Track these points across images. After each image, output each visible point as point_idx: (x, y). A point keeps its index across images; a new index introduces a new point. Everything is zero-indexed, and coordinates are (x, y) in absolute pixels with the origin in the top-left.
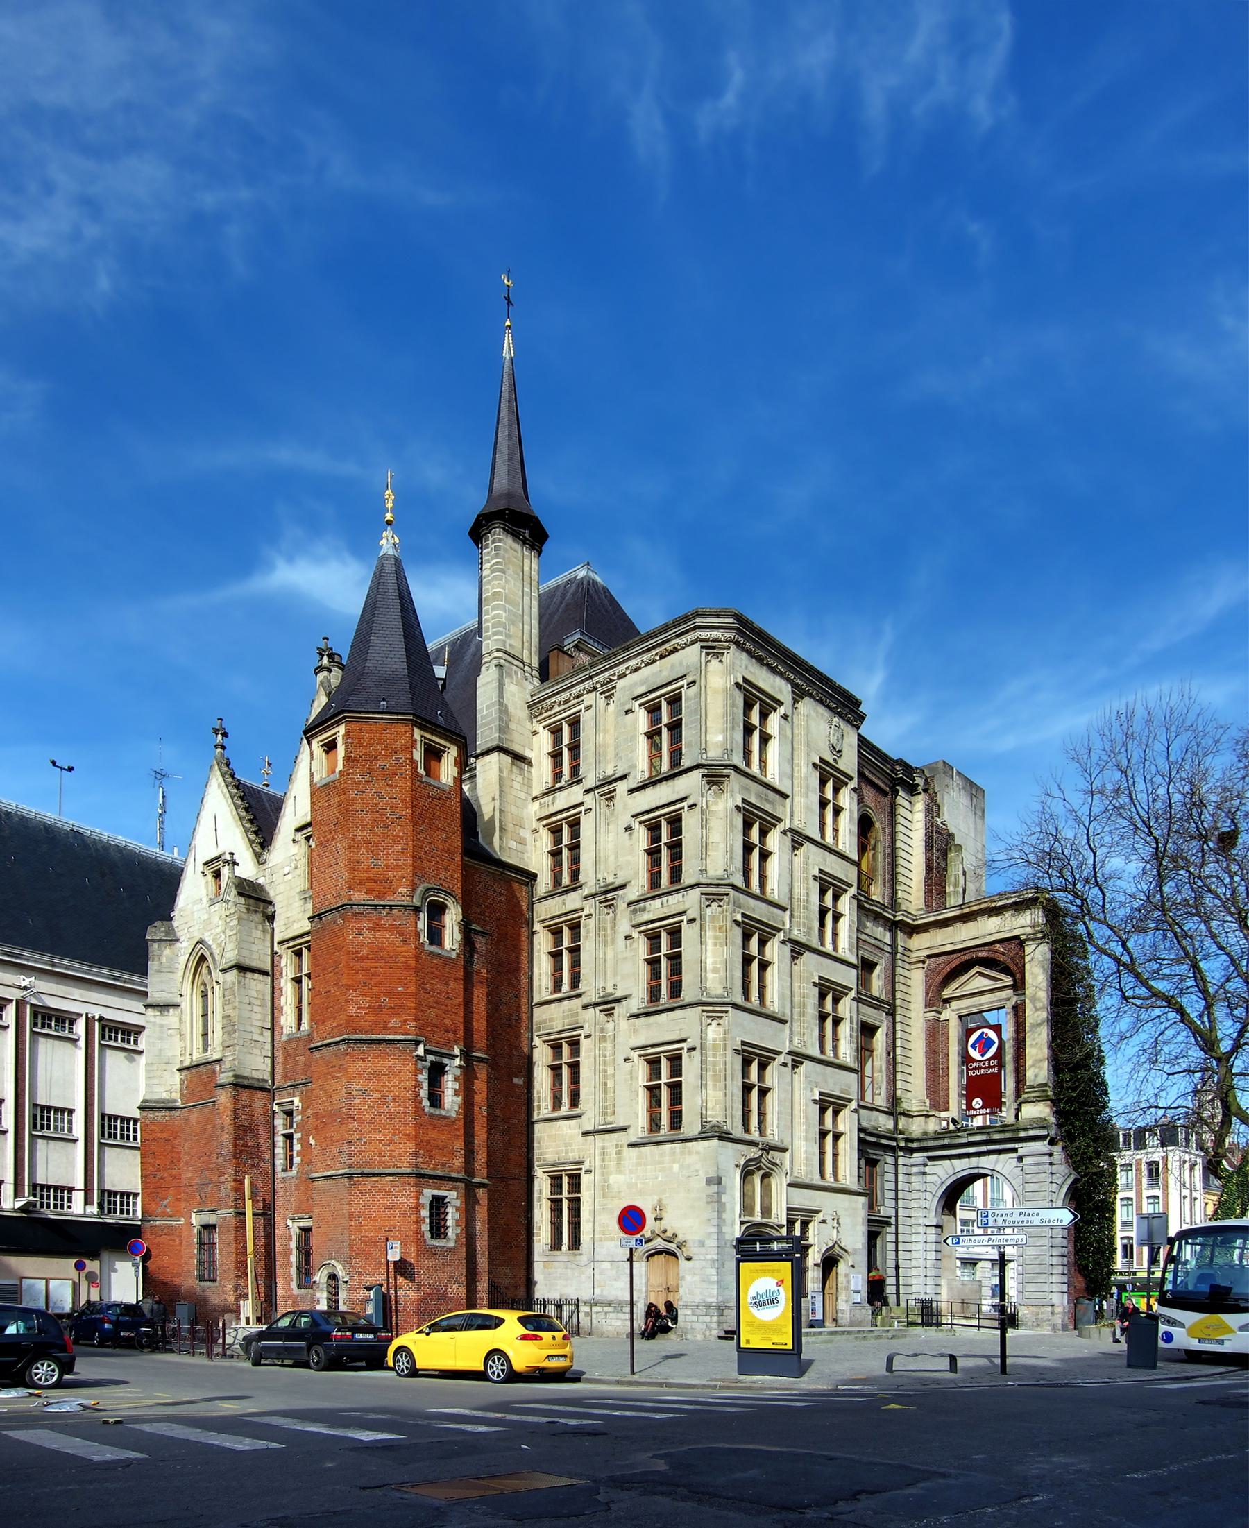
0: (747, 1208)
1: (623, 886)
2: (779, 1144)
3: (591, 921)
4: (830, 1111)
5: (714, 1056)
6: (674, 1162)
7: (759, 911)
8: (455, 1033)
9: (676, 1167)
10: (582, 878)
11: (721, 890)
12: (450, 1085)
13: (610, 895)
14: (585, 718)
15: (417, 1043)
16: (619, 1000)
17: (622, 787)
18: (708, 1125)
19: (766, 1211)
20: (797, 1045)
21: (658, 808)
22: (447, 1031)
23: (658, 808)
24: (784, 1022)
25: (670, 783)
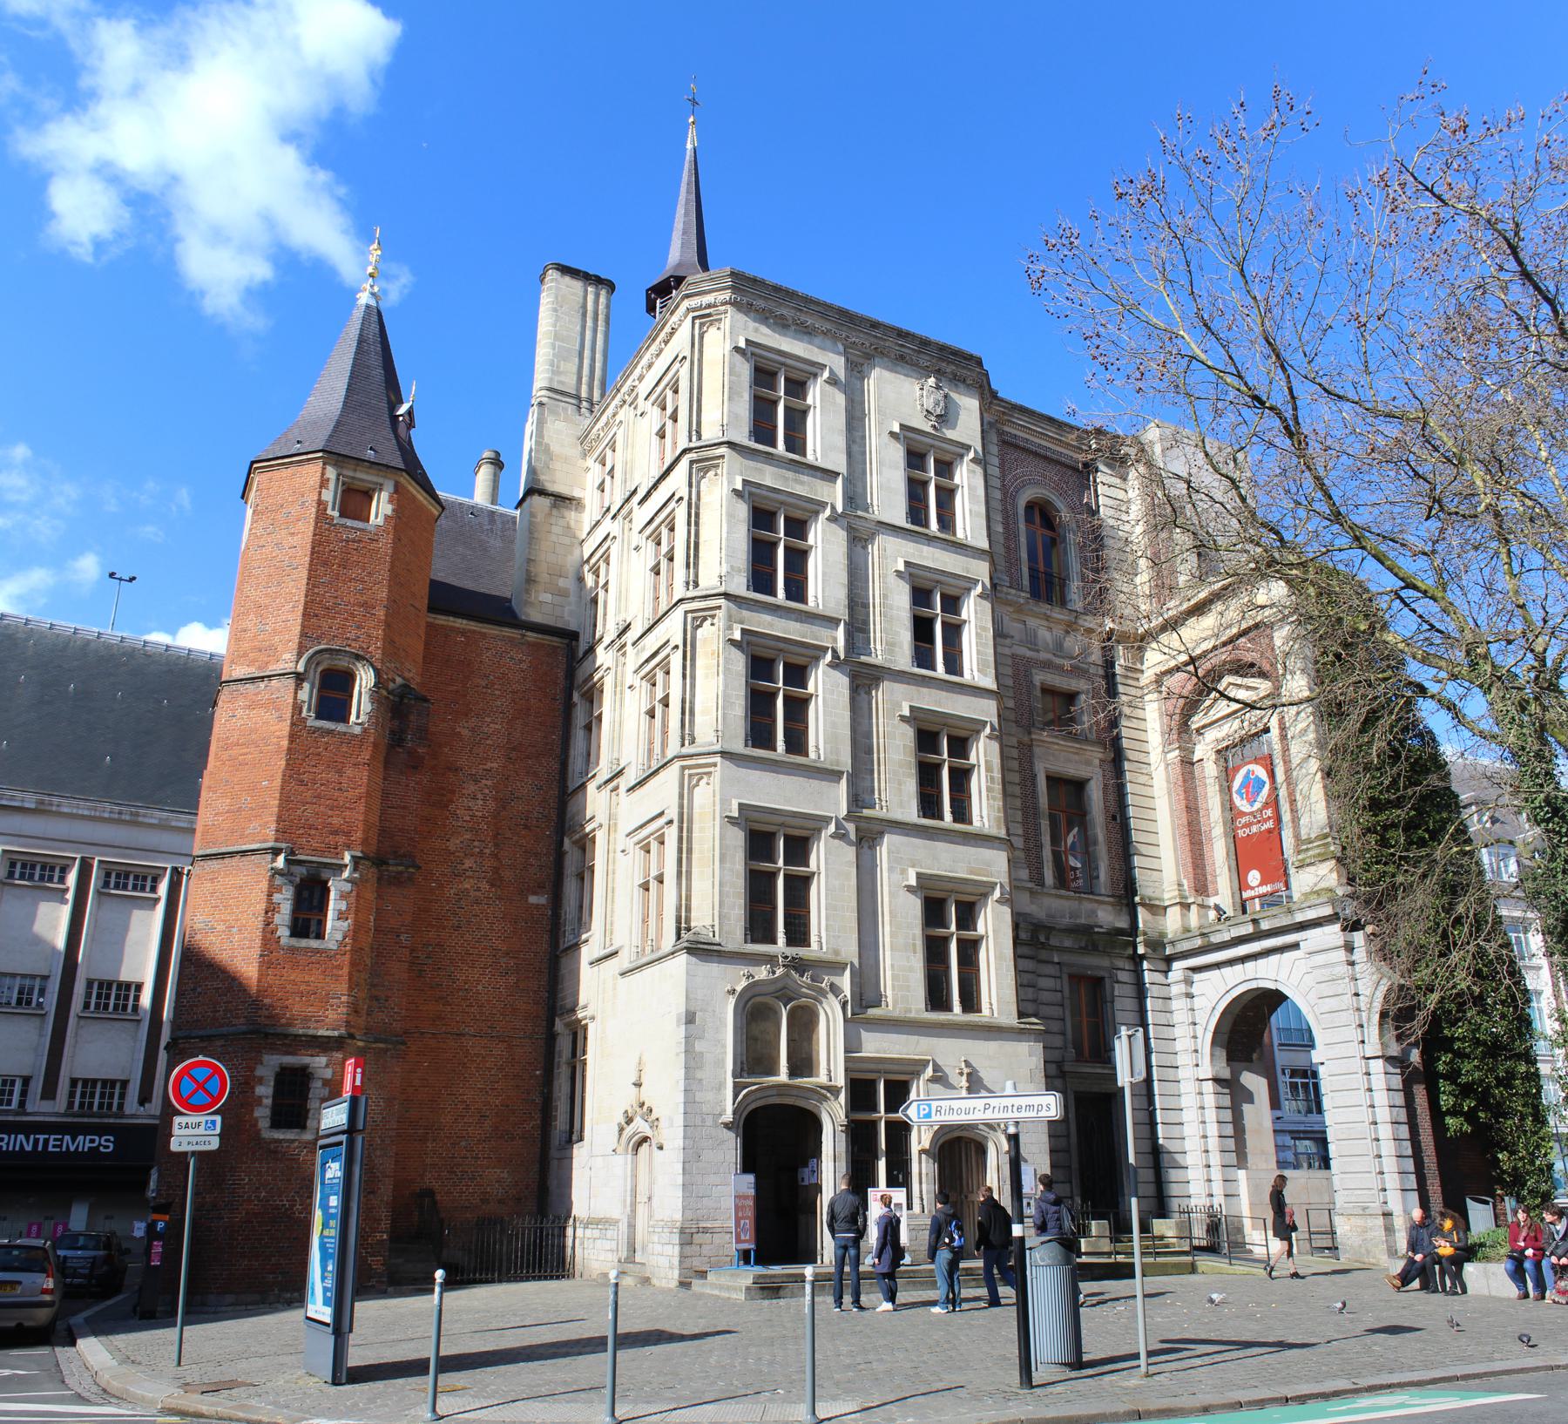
0: (754, 1058)
2: (830, 957)
8: (348, 834)
15: (276, 852)
19: (802, 1063)
22: (335, 833)
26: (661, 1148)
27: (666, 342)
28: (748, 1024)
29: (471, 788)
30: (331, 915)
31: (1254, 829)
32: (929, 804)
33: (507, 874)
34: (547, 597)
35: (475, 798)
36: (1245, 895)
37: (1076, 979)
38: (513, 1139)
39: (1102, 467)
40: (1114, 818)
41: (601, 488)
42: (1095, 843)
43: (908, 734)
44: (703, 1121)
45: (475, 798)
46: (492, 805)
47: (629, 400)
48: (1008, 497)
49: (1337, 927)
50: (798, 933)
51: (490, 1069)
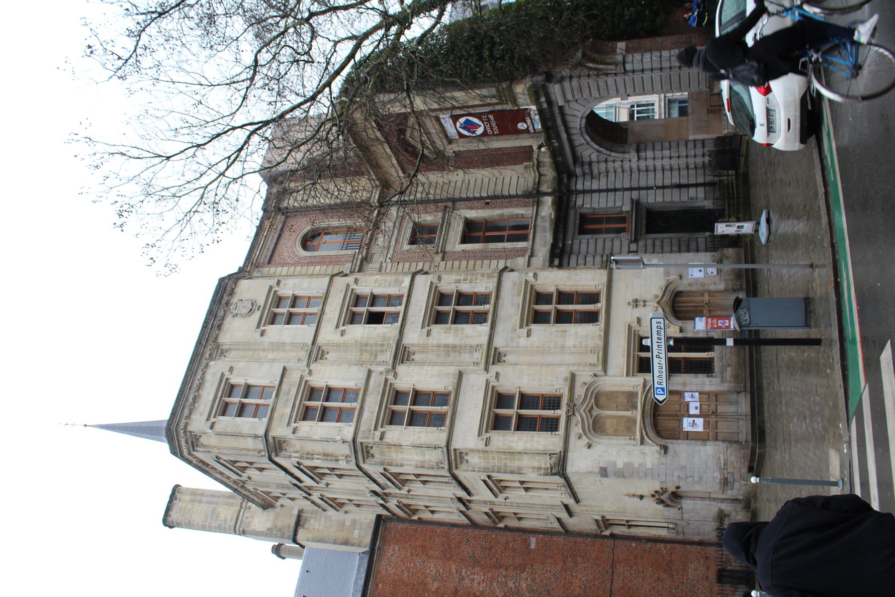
20: (480, 356)
24: (461, 375)
26: (678, 487)
28: (607, 434)
29: (467, 582)
32: (479, 318)
33: (518, 561)
35: (473, 580)
36: (532, 131)
37: (582, 231)
38: (671, 561)
39: (286, 205)
40: (488, 203)
41: (292, 499)
42: (502, 215)
43: (436, 329)
44: (662, 464)
45: (473, 580)
46: (477, 569)
47: (241, 484)
48: (299, 262)
50: (553, 402)
51: (631, 574)
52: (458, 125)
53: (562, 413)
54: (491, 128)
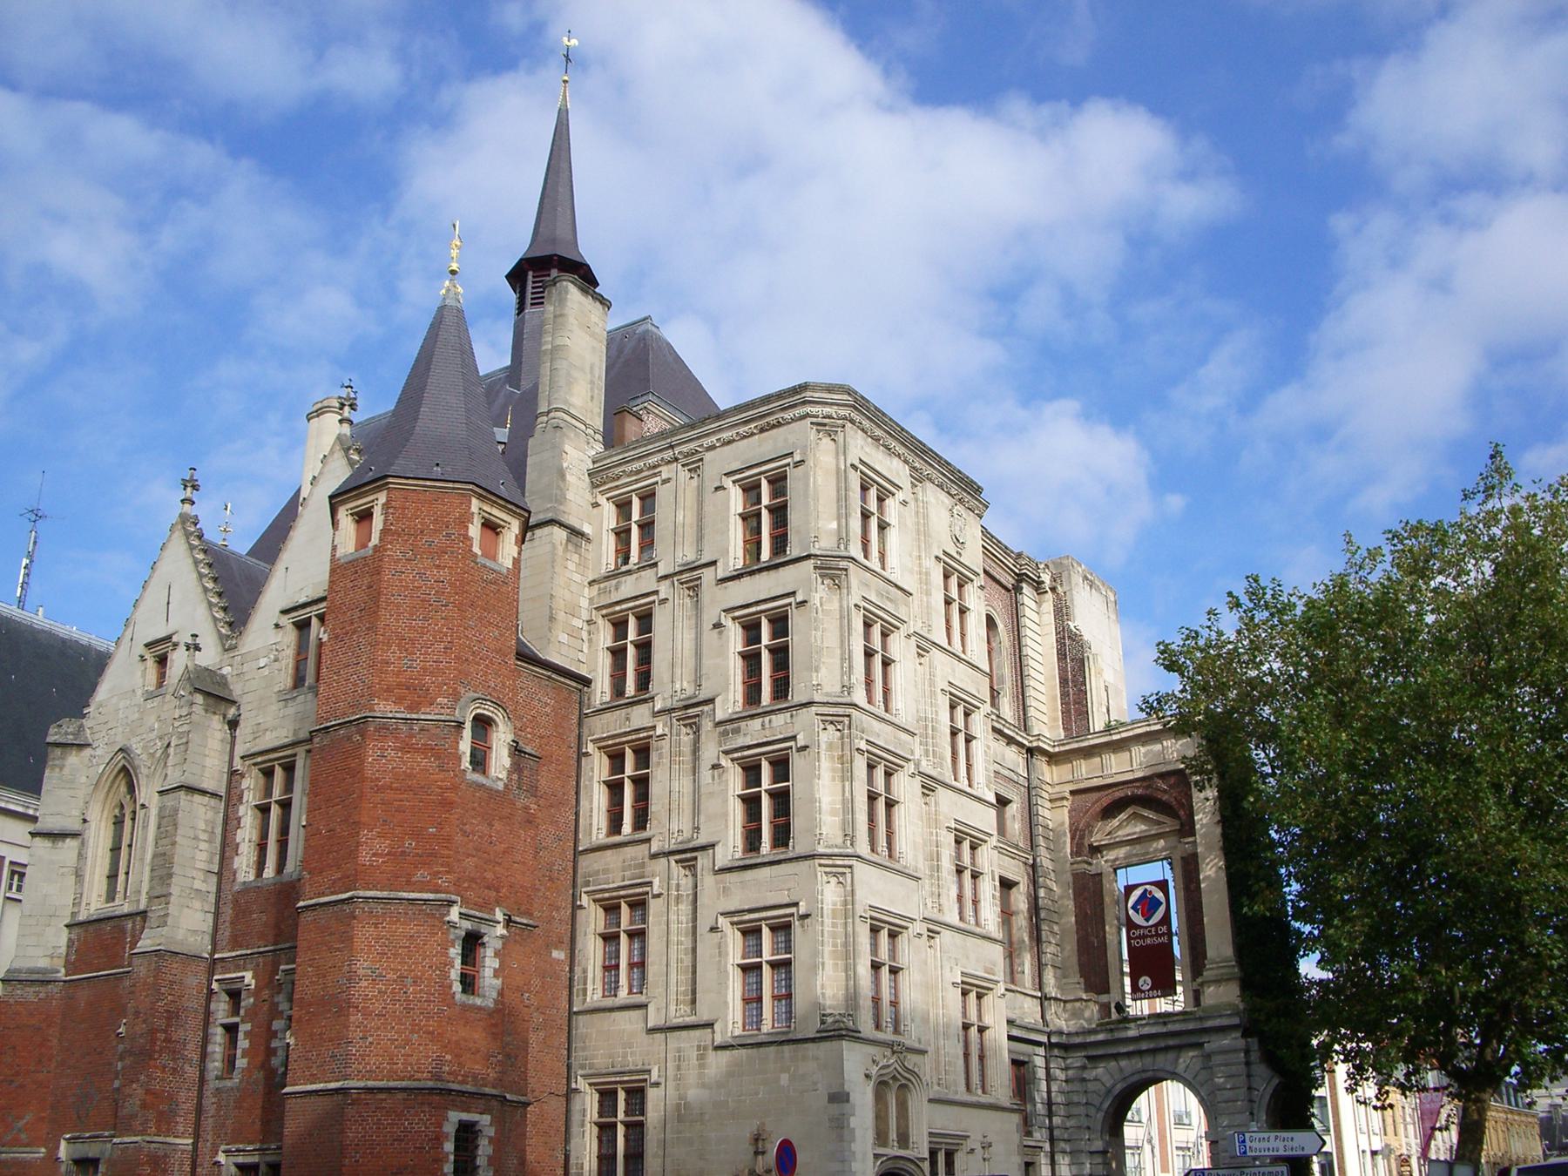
1: (711, 701)
3: (665, 743)
4: (973, 996)
5: (834, 925)
6: (783, 1070)
7: (884, 735)
9: (784, 1079)
10: (654, 687)
11: (840, 711)
12: (488, 962)
13: (691, 711)
14: (663, 493)
15: (451, 903)
16: (703, 848)
17: (708, 575)
18: (830, 1020)
19: (904, 1140)
21: (757, 603)
22: (488, 888)
23: (757, 603)
25: (772, 573)
27: (762, 430)
30: (488, 972)
31: (1148, 941)
34: (564, 638)
49: (1238, 1034)
52: (1152, 888)
53: (887, 1035)
54: (1143, 937)
